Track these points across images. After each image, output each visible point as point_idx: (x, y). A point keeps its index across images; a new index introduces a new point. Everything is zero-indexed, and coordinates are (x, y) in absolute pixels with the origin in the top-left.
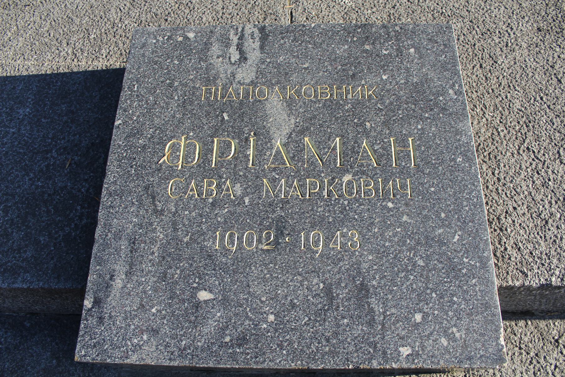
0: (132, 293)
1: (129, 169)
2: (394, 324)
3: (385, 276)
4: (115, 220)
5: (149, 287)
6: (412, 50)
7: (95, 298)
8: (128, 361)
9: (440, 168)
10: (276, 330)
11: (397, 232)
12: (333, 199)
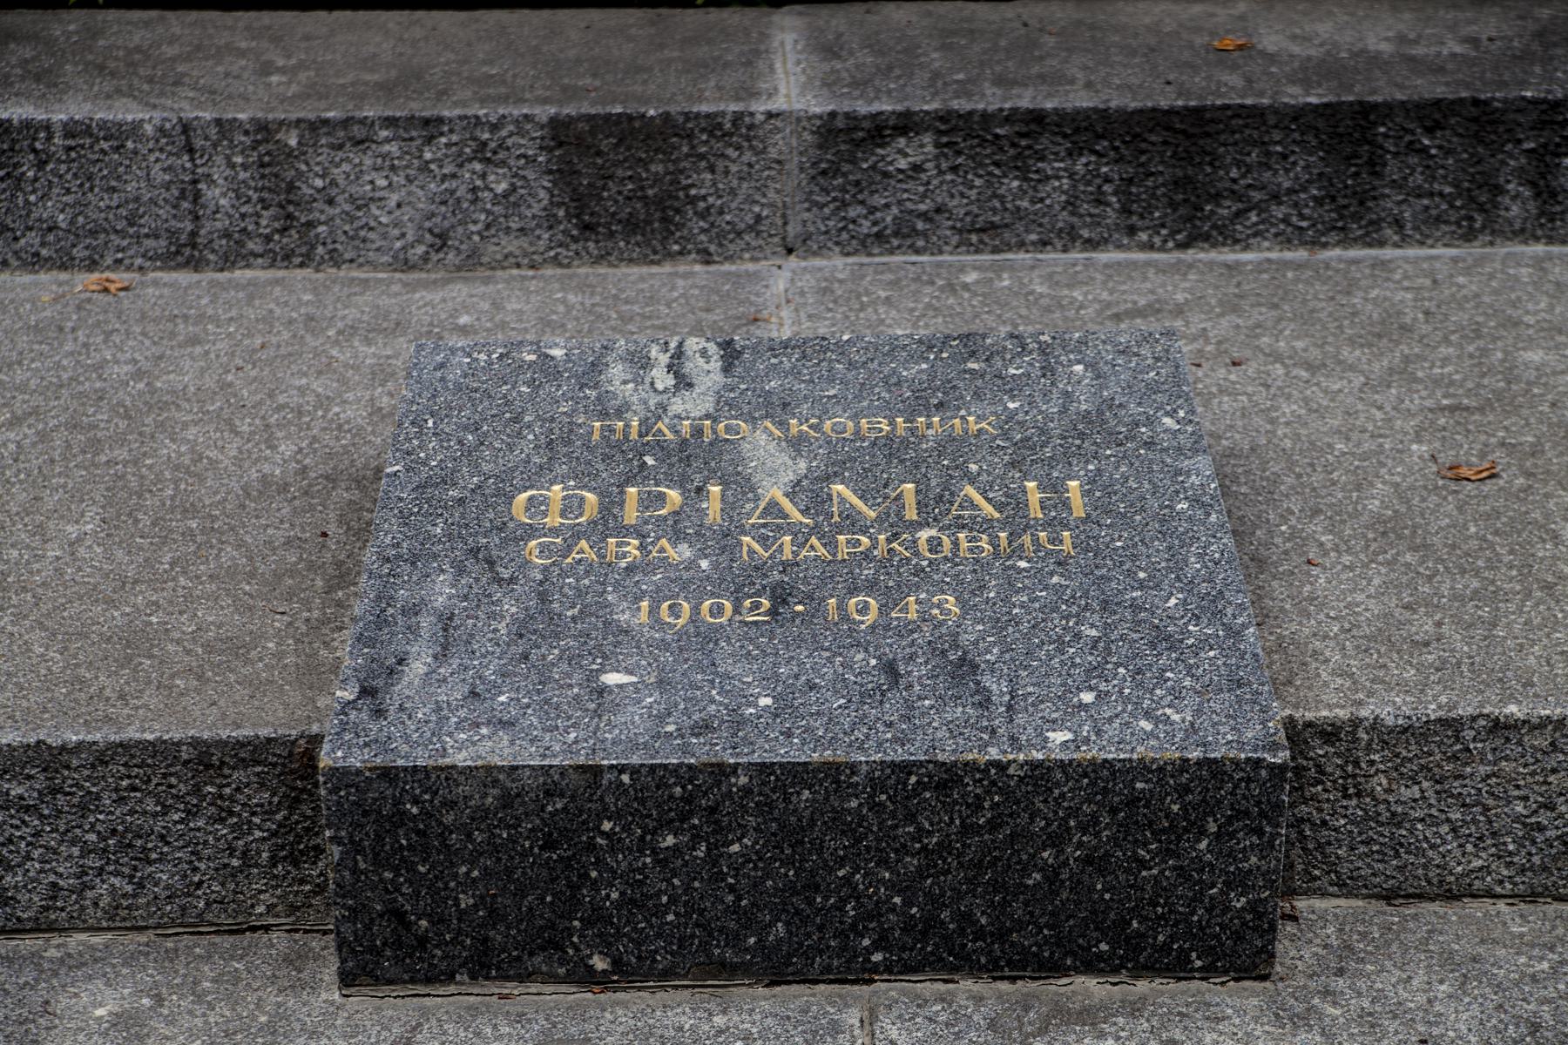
2: (1033, 705)
6: (1079, 368)
8: (447, 761)
9: (1138, 518)
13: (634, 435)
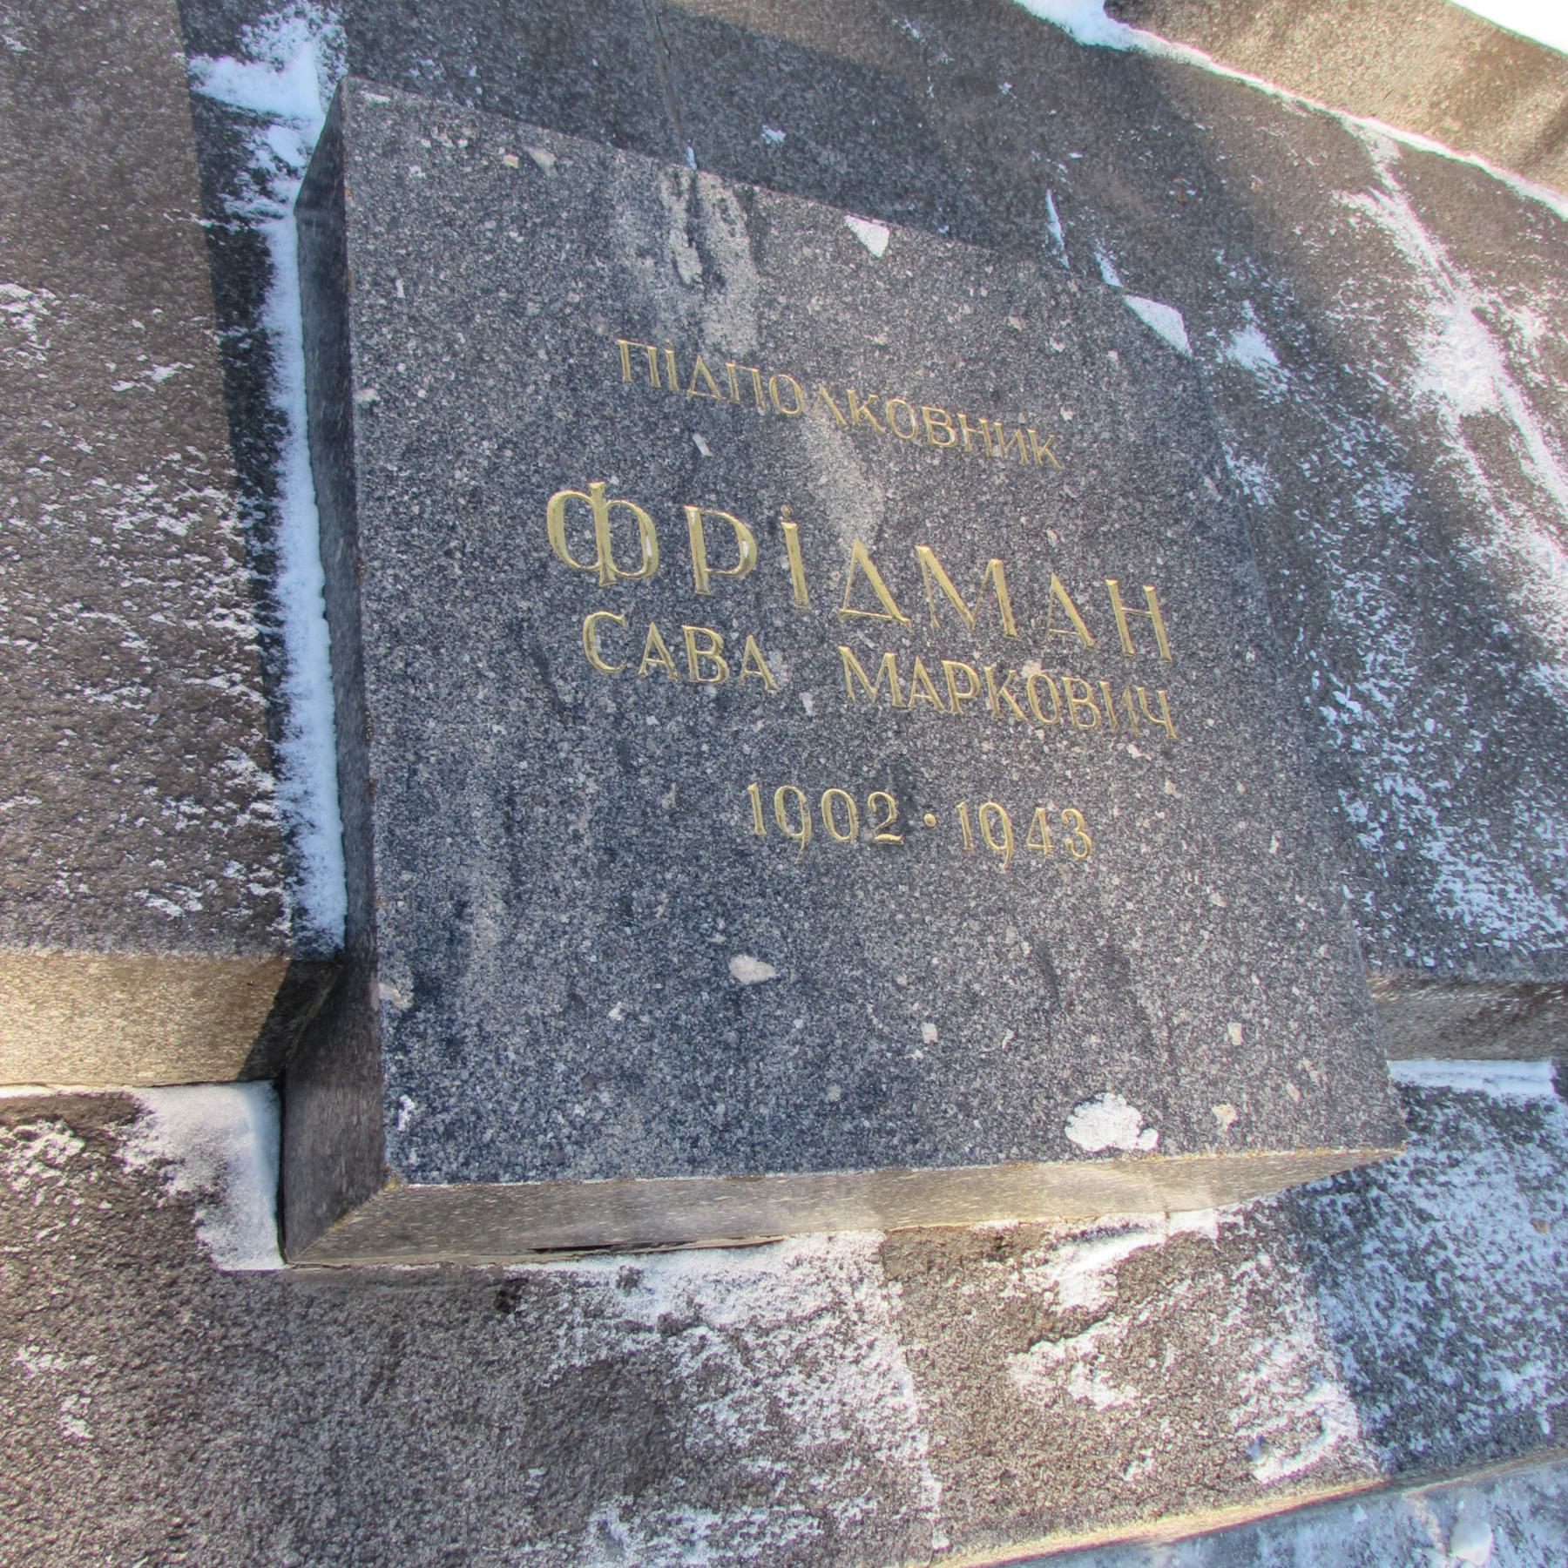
0: (537, 960)
1: (443, 561)
3: (1154, 929)
4: (432, 724)
5: (588, 943)
7: (418, 976)
9: (1217, 671)
10: (947, 1066)
11: (1159, 821)
12: (1011, 721)
13: (673, 383)
